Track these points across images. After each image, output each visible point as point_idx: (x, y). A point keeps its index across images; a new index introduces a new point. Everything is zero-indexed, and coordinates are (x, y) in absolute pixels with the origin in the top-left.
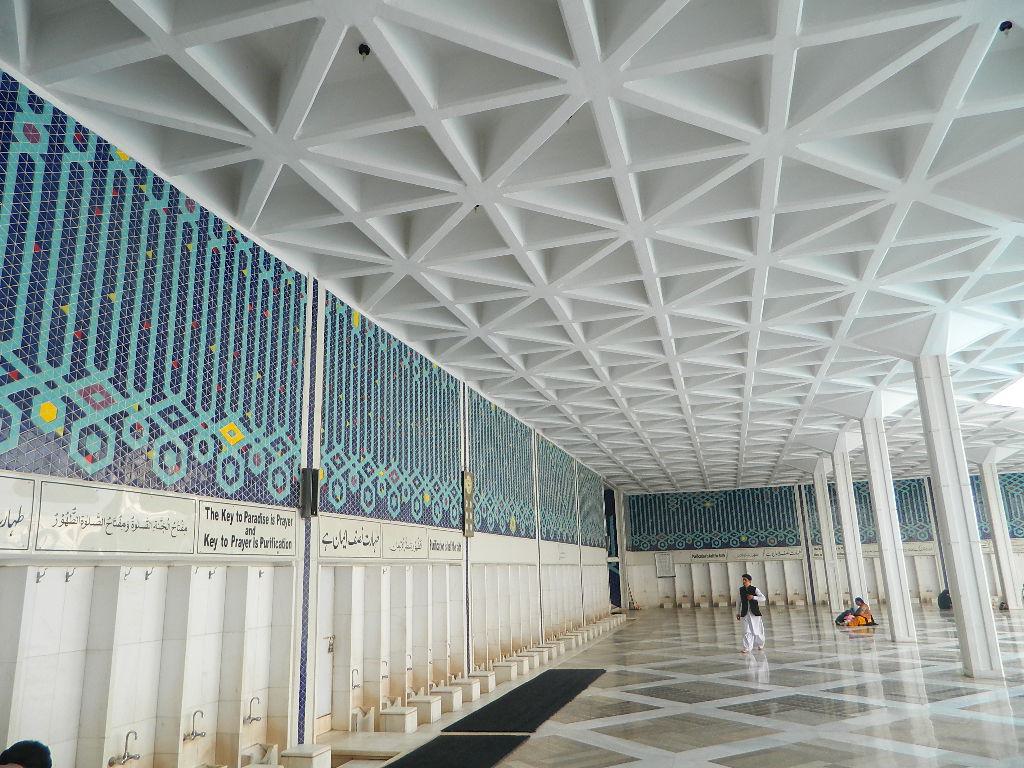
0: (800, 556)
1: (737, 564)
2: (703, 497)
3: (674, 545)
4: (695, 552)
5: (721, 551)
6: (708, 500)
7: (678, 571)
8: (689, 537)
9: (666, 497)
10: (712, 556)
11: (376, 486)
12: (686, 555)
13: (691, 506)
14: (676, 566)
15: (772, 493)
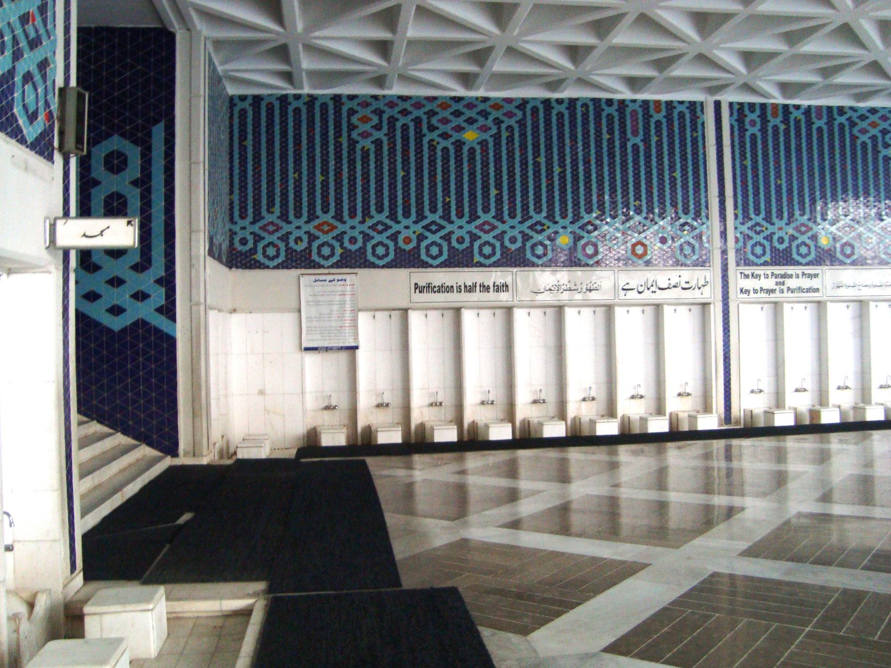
0: (706, 294)
1: (537, 313)
2: (457, 114)
3: (362, 250)
5: (497, 276)
6: (471, 121)
7: (371, 334)
8: (408, 229)
10: (470, 289)
12: (396, 283)
13: (419, 136)
14: (363, 319)
15: (647, 116)
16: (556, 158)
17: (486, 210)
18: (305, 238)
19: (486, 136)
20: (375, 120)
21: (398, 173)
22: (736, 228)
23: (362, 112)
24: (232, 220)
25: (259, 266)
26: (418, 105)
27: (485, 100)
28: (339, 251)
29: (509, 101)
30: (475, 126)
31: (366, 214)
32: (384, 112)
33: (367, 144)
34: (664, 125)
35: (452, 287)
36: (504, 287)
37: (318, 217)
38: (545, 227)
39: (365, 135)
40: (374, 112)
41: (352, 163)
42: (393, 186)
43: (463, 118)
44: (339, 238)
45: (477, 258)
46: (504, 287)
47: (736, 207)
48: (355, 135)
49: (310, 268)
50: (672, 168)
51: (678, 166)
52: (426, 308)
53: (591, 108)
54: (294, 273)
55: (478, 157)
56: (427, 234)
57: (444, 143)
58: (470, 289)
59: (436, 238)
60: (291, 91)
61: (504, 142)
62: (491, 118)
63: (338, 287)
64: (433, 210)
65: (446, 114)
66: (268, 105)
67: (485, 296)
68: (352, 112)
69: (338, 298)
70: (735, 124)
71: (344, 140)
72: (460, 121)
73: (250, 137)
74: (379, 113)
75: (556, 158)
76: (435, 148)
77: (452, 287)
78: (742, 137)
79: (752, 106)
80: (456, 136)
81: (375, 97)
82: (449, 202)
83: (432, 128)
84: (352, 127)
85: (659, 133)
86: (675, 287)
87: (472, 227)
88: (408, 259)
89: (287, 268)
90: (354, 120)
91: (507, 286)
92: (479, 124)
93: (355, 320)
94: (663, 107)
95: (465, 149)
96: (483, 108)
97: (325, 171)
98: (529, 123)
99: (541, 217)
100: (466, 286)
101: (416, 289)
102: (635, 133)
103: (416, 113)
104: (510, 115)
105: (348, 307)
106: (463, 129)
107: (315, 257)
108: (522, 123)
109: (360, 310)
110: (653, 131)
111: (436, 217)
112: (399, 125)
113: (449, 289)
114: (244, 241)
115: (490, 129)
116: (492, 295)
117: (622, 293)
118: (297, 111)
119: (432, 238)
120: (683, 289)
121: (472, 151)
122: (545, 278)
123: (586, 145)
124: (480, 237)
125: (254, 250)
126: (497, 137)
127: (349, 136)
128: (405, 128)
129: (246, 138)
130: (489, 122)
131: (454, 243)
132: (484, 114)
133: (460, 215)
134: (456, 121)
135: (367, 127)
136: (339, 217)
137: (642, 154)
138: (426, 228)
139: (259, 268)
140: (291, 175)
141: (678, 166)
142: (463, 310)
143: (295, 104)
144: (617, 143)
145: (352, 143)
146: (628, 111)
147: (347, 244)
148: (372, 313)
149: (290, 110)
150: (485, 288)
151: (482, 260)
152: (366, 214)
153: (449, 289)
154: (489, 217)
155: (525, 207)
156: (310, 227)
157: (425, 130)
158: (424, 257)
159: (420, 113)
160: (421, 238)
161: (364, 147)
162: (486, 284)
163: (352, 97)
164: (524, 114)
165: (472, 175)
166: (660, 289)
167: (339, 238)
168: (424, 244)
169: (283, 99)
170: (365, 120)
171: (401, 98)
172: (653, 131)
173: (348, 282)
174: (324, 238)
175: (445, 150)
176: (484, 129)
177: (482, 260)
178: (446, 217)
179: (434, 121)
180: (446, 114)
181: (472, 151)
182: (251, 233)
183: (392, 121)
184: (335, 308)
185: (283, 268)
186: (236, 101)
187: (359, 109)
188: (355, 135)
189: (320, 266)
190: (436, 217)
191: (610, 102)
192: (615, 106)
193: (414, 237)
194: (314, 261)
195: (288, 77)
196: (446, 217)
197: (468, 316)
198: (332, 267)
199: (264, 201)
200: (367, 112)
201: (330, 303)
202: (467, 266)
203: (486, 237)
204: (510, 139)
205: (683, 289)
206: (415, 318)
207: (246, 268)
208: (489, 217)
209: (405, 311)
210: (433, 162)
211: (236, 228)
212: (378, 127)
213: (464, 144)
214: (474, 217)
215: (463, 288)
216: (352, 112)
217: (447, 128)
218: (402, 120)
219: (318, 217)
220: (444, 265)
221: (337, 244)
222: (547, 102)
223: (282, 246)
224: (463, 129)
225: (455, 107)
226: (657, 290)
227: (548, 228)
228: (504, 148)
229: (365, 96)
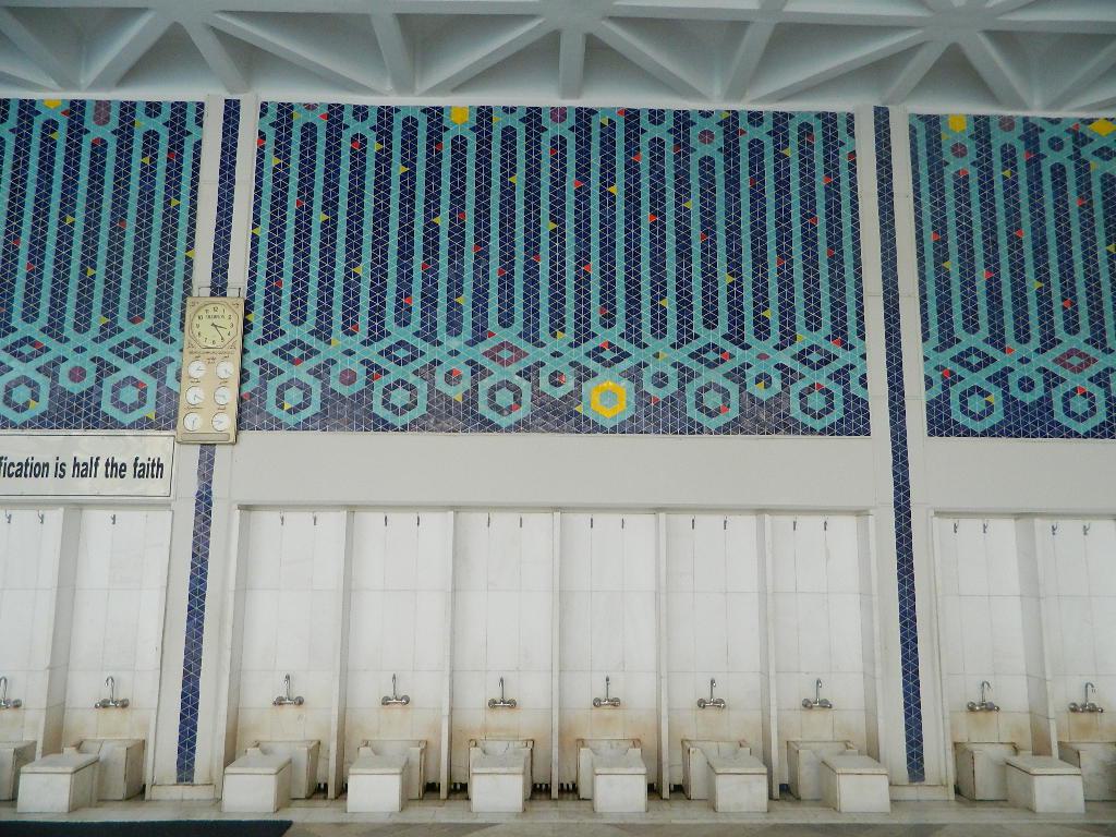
10: (84, 470)
35: (47, 465)
58: (84, 470)
67: (115, 486)
77: (47, 465)
91: (160, 466)
100: (76, 465)
113: (39, 470)
153: (39, 470)
158: (107, 407)
162: (119, 461)
215: (69, 469)
220: (44, 422)
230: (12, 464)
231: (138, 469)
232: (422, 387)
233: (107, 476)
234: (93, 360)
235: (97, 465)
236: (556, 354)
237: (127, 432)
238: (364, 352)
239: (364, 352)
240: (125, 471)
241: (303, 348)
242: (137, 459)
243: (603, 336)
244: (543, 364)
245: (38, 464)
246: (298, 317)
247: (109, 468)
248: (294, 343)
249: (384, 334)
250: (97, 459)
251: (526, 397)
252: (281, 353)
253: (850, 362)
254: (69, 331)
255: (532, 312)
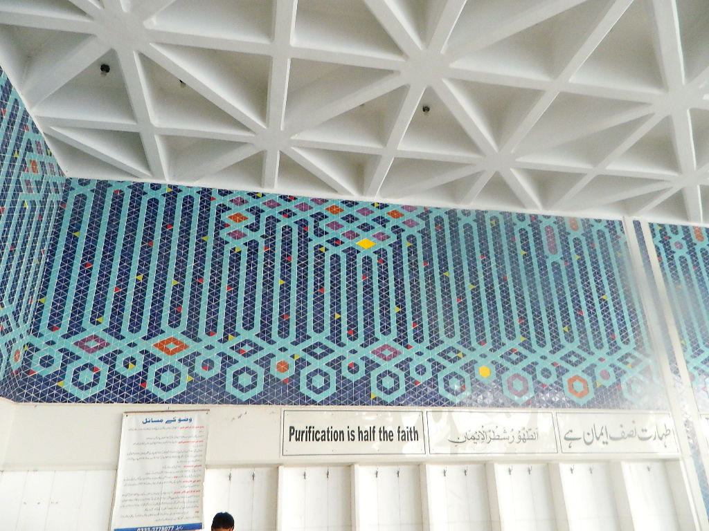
1: (455, 471)
2: (350, 219)
4: (302, 417)
5: (409, 417)
6: (366, 228)
8: (284, 353)
9: (218, 200)
10: (366, 436)
11: (9, 351)
15: (564, 235)
16: (466, 273)
17: (386, 330)
18: (140, 359)
19: (385, 245)
20: (251, 219)
21: (275, 281)
22: (687, 362)
23: (236, 209)
24: (35, 331)
25: (65, 397)
26: (304, 207)
27: (383, 206)
28: (186, 379)
29: (410, 209)
30: (371, 232)
31: (230, 329)
32: (263, 211)
33: (240, 245)
34: (584, 244)
35: (342, 432)
36: (410, 435)
37: (162, 332)
38: (460, 355)
39: (237, 235)
40: (251, 210)
41: (217, 266)
42: (267, 298)
43: (357, 224)
44: (189, 361)
45: (375, 393)
46: (410, 435)
47: (682, 338)
48: (223, 234)
49: (142, 401)
50: (600, 289)
51: (607, 288)
52: (305, 464)
53: (501, 222)
54: (117, 408)
55: (375, 269)
56: (309, 358)
57: (333, 250)
58: (366, 436)
59: (321, 364)
60: (148, 180)
61: (405, 253)
62: (389, 226)
63: (179, 431)
64: (319, 328)
65: (337, 218)
66: (115, 193)
68: (223, 208)
69: (177, 447)
70: (660, 245)
71: (210, 239)
72: (353, 227)
73: (85, 227)
74: (257, 212)
75: (466, 273)
76: (324, 255)
77: (342, 432)
78: (671, 259)
79: (674, 229)
80: (349, 243)
81: (253, 195)
82: (340, 319)
83: (319, 233)
84: (220, 225)
85: (579, 250)
86: (630, 436)
87: (368, 352)
88: (284, 392)
89: (106, 401)
90: (225, 217)
91: (416, 432)
92: (376, 232)
93: (199, 481)
94: (580, 224)
95: (359, 258)
96: (381, 216)
97: (180, 275)
98: (433, 234)
99: (454, 342)
100: (360, 432)
101: (291, 434)
102: (553, 250)
103: (301, 215)
104: (411, 224)
105: (191, 460)
106: (358, 235)
107: (150, 386)
108: (425, 234)
109: (207, 467)
110: (572, 250)
111: (322, 338)
112: (279, 226)
113: (338, 436)
114: (47, 361)
115: (388, 237)
116: (394, 445)
117: (566, 444)
118: (153, 203)
119: (316, 364)
120: (641, 439)
121: (367, 261)
122: (467, 420)
123: (500, 261)
124: (378, 365)
125: (61, 374)
126: (397, 247)
127: (217, 234)
128: (287, 231)
129: (79, 228)
130: (388, 230)
131: (345, 373)
132: (382, 221)
133: (353, 336)
134: (348, 227)
135: (241, 226)
136: (192, 333)
137: (564, 273)
138: (308, 351)
139: (63, 400)
140: (133, 277)
141: (607, 288)
142: (356, 467)
143: (152, 194)
144: (535, 260)
145: (220, 244)
146: (542, 227)
147: (198, 369)
148: (226, 472)
149: (145, 199)
150: (387, 436)
151: (382, 395)
152: (230, 329)
153: (338, 436)
154: (389, 340)
155: (434, 330)
156: (150, 346)
157: (311, 234)
159: (306, 215)
160: (301, 364)
161: (234, 249)
163: (224, 193)
164: (427, 224)
165: (368, 288)
166: (611, 438)
167: (189, 361)
168: (305, 372)
169: (137, 189)
170: (238, 218)
171: (283, 197)
172: (572, 250)
173: (195, 423)
174: (167, 360)
175: (336, 258)
176: (382, 237)
177: (382, 395)
178: (336, 337)
179: (323, 225)
180: (337, 218)
181: (367, 261)
182: (61, 351)
183: (272, 221)
184: (172, 462)
185: (101, 401)
186: (75, 184)
187: (232, 205)
188: (223, 234)
189: (157, 400)
190: (322, 338)
191: (521, 217)
192: (528, 221)
193: (292, 362)
194: (148, 392)
195: (133, 142)
196: (336, 337)
197: (363, 475)
198: (173, 401)
199: (89, 308)
200: (242, 210)
201: (166, 455)
202: (362, 403)
203: (386, 366)
204: (412, 251)
205: (641, 439)
206: (289, 479)
207: (44, 400)
208: (389, 340)
209: (274, 470)
210: (319, 271)
211: (37, 342)
212: (254, 228)
213: (358, 252)
214: (370, 339)
215: (356, 434)
216: (223, 208)
217: (339, 234)
218: (284, 222)
219: (162, 332)
221: (184, 370)
222: (452, 214)
223: (104, 369)
224: (358, 235)
225: (348, 211)
226: (609, 440)
227: (464, 355)
228: (405, 259)
229: (241, 192)
230: (318, 432)
231: (401, 435)
232: (401, 375)
233: (381, 440)
234: (61, 351)
235: (374, 432)
236: (601, 360)
237: (389, 408)
238: (144, 345)
239: (144, 345)
240: (393, 435)
241: (251, 345)
242: (399, 427)
243: (383, 340)
244: (411, 360)
245: (336, 432)
246: (249, 325)
247: (382, 434)
248: (512, 350)
249: (561, 347)
250: (374, 427)
251: (333, 379)
252: (442, 355)
253: (534, 361)
254: (345, 339)
255: (495, 328)
